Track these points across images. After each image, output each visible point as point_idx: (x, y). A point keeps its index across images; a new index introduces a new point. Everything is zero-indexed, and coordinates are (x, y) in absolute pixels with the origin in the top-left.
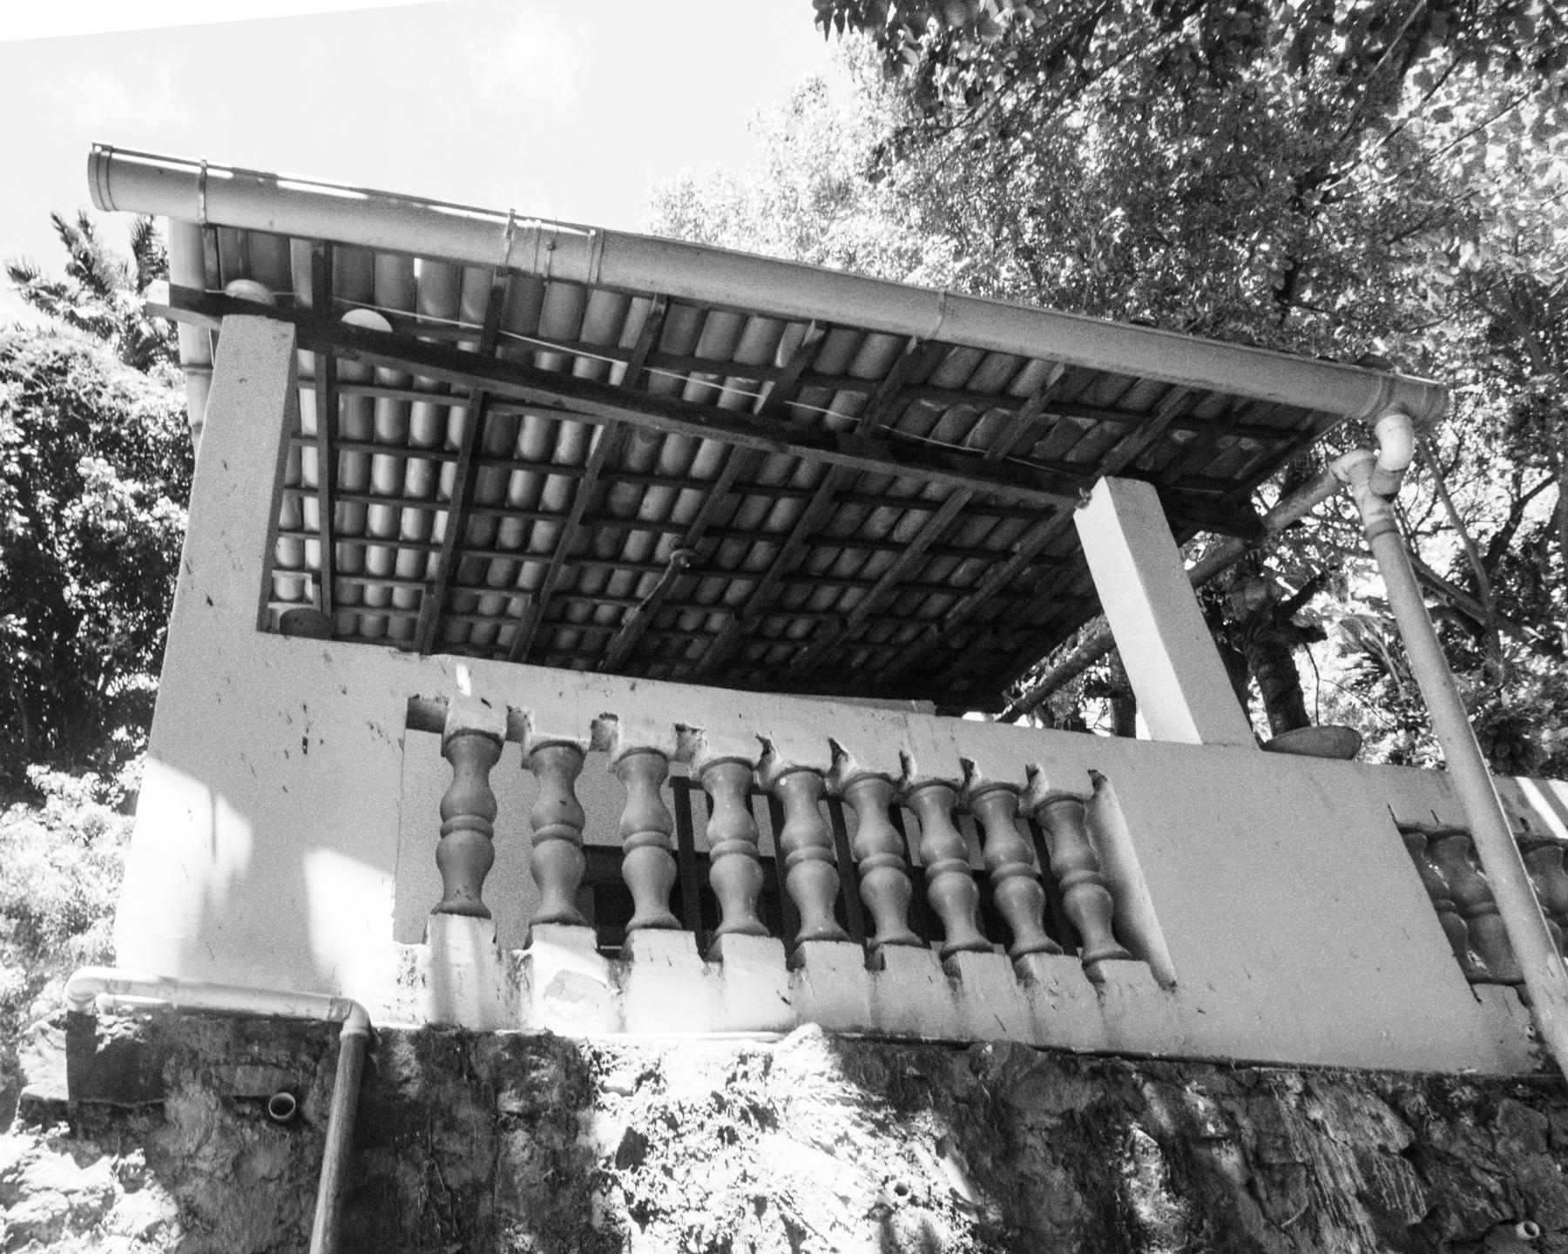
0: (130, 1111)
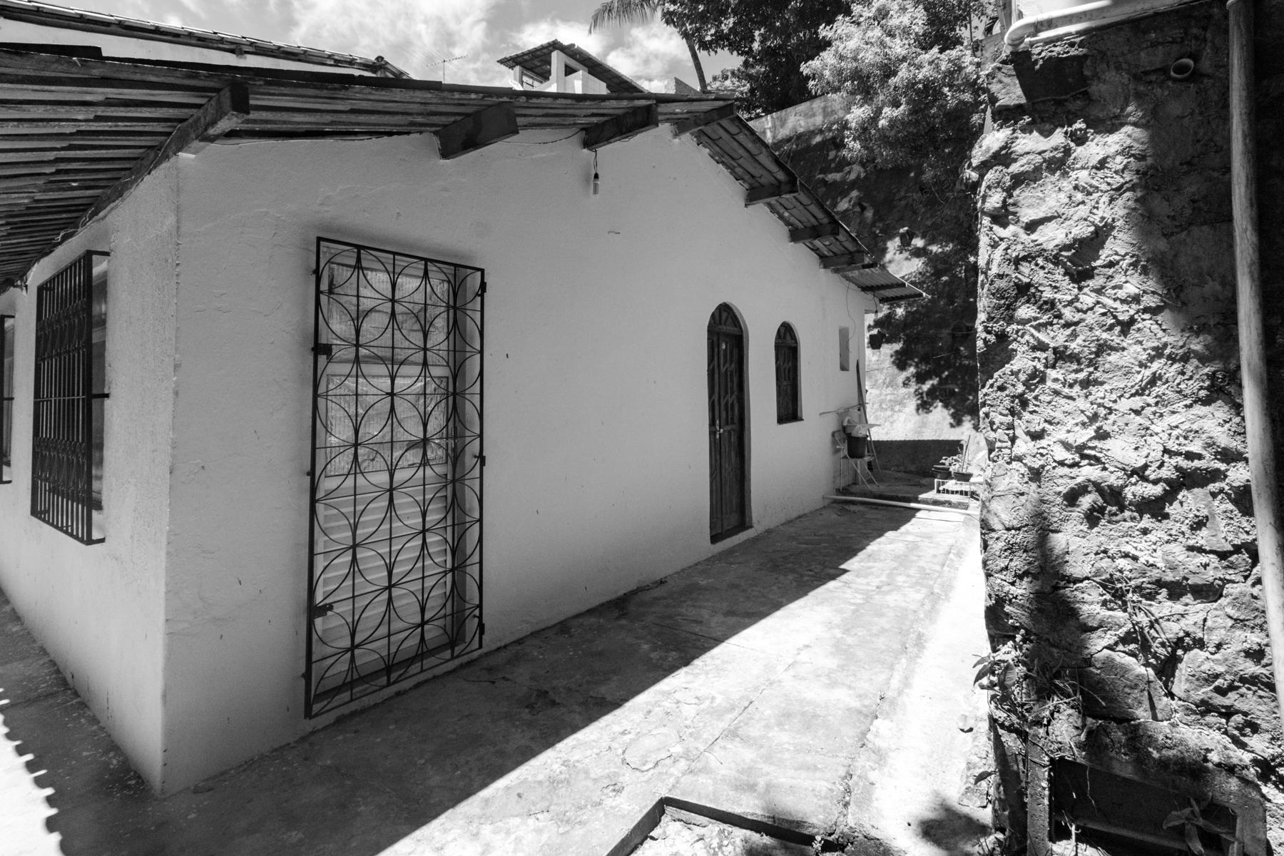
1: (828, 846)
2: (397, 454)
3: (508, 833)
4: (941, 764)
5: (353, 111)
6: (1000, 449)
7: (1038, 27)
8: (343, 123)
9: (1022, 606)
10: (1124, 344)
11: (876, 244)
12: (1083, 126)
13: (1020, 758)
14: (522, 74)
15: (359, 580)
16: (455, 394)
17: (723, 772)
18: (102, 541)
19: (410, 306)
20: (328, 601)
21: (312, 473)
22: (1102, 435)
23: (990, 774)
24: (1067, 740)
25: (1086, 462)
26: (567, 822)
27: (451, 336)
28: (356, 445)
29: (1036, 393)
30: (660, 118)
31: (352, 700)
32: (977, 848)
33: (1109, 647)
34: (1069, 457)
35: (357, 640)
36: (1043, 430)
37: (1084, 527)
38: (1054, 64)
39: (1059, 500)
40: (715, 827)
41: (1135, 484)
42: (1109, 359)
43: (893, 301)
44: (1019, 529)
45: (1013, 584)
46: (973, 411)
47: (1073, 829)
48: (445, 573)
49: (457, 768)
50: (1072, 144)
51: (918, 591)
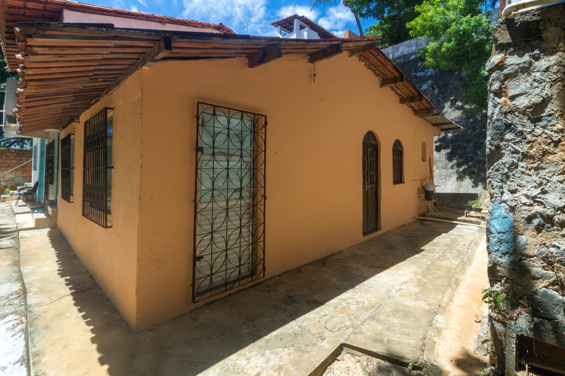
0: (530, 40)
1: (415, 368)
2: (229, 194)
3: (277, 354)
4: (466, 335)
5: (213, 48)
6: (496, 197)
7: (518, 7)
8: (209, 53)
9: (505, 267)
10: (556, 151)
11: (439, 104)
12: (538, 52)
13: (502, 334)
15: (214, 246)
16: (254, 169)
17: (368, 334)
18: (111, 227)
19: (235, 131)
20: (201, 255)
21: (195, 201)
22: (544, 192)
23: (488, 341)
24: (525, 327)
25: (536, 204)
26: (302, 351)
27: (252, 144)
28: (213, 190)
29: (513, 172)
30: (343, 49)
31: (211, 296)
32: (482, 372)
33: (545, 287)
34: (528, 201)
35: (213, 272)
36: (516, 189)
37: (535, 233)
38: (526, 24)
39: (523, 221)
40: (365, 357)
41: (559, 214)
42: (549, 158)
43: (446, 130)
44: (504, 233)
45: (501, 257)
46: (484, 180)
47: (527, 366)
48: (249, 245)
49: (254, 326)
50: (533, 61)
51: (456, 260)
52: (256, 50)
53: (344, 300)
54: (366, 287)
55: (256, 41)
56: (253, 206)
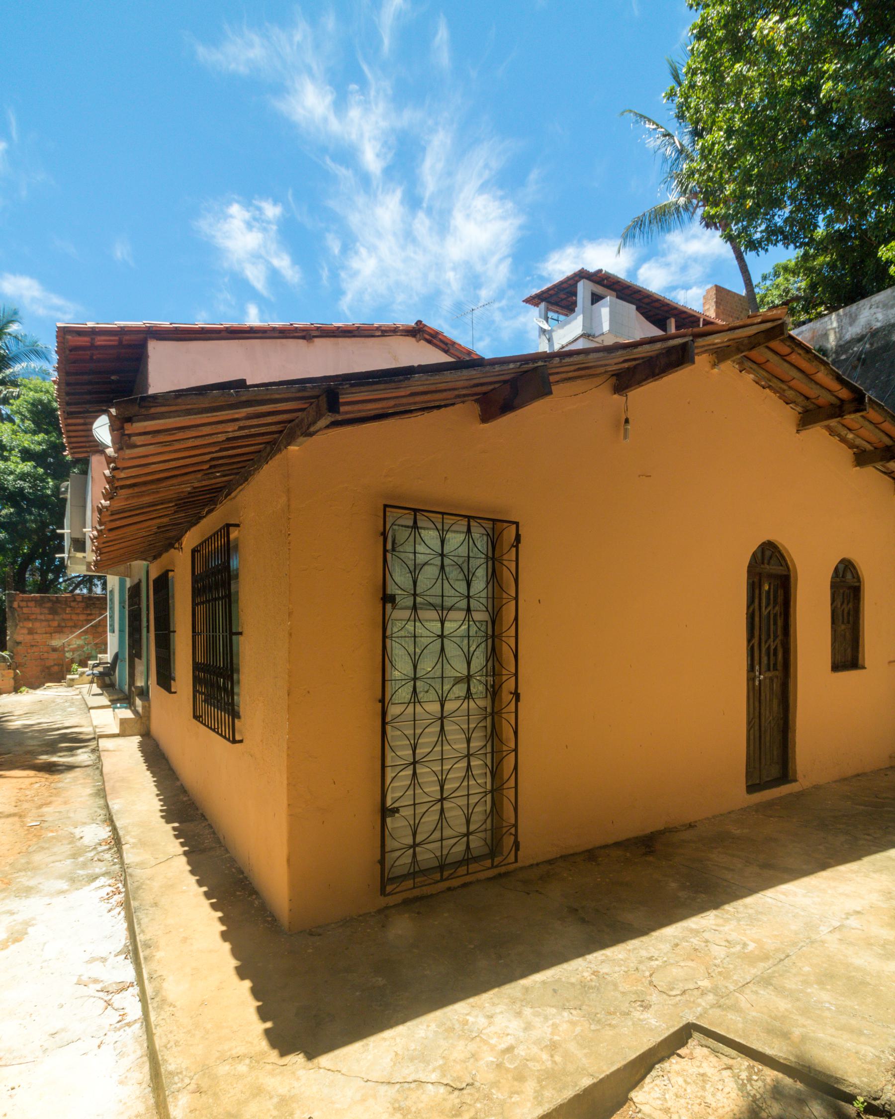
14: (547, 310)
16: (493, 636)
19: (455, 559)
31: (414, 888)
35: (418, 840)
52: (497, 386)
53: (696, 932)
54: (751, 911)
55: (497, 368)
56: (494, 715)
